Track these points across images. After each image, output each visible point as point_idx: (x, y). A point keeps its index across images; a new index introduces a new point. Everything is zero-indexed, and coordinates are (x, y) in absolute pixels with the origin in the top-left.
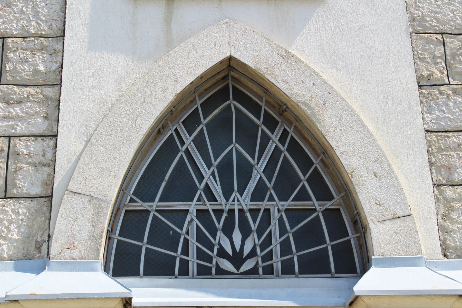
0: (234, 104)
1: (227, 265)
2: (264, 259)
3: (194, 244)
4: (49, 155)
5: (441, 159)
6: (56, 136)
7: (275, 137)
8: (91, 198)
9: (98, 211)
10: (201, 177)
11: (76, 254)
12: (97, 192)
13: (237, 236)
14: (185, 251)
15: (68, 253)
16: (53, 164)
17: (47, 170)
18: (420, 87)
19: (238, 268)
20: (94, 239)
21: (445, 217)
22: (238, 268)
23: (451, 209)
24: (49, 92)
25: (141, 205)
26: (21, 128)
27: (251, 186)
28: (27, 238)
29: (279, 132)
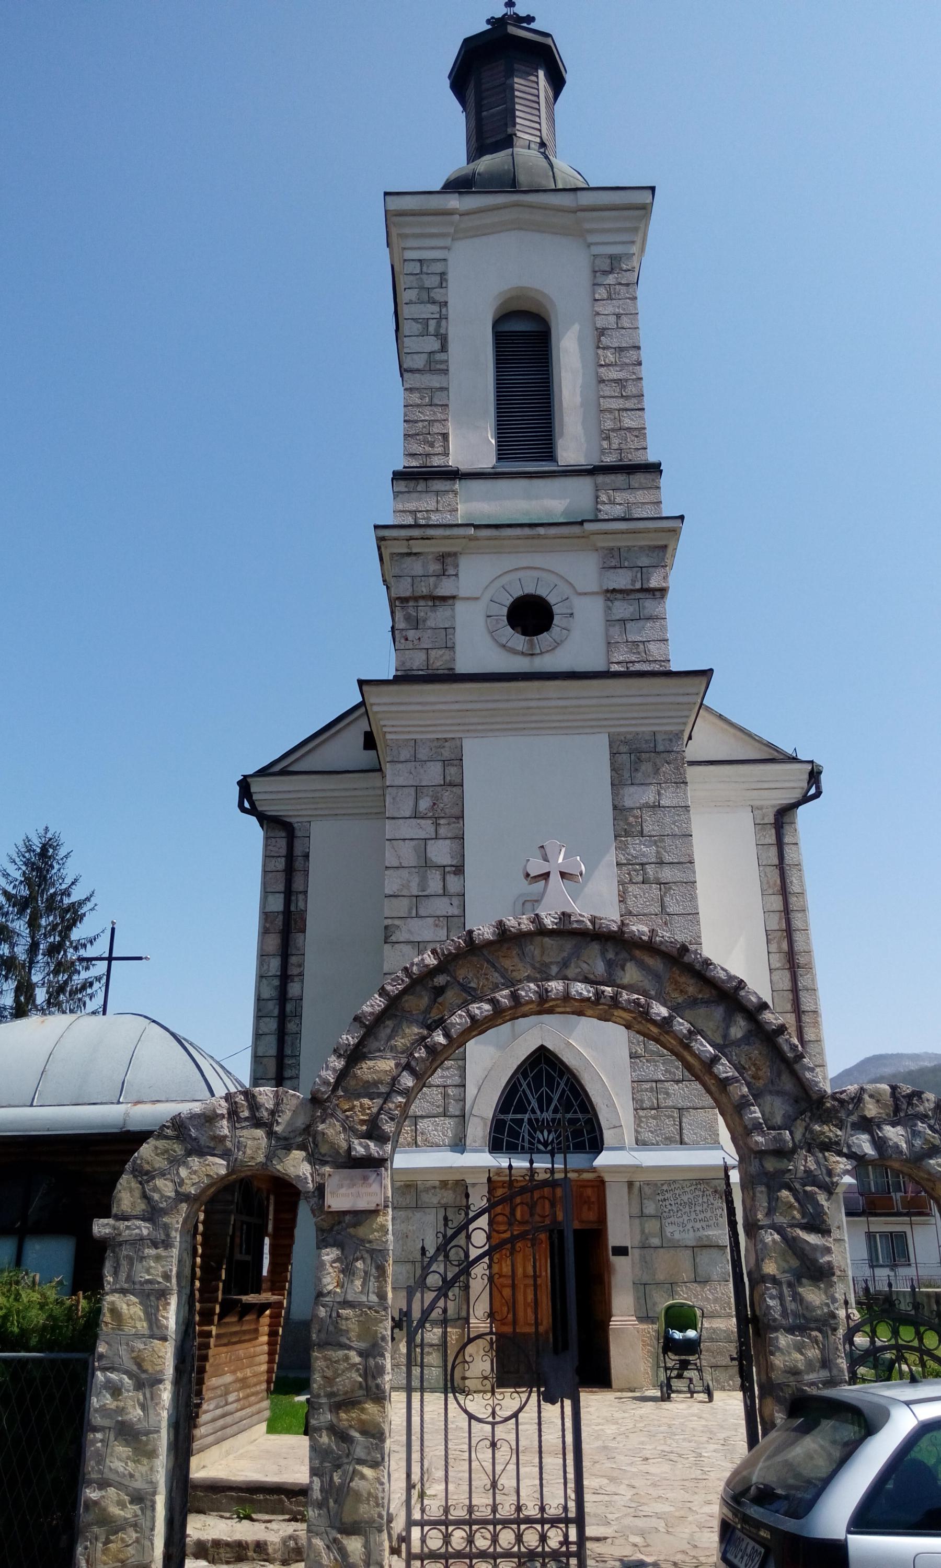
0: (544, 1066)
1: (541, 1147)
2: (558, 1144)
3: (526, 1136)
4: (462, 1095)
5: (638, 1096)
6: (464, 1086)
7: (562, 1085)
8: (482, 1118)
9: (485, 1125)
10: (529, 1103)
11: (477, 1144)
12: (485, 1116)
13: (546, 1133)
14: (523, 1141)
15: (474, 1144)
16: (464, 1100)
17: (462, 1103)
18: (631, 1058)
19: (546, 1148)
20: (484, 1137)
21: (639, 1125)
22: (546, 1148)
23: (642, 1122)
24: (460, 1063)
25: (502, 1117)
26: (449, 1082)
27: (552, 1107)
28: (455, 1135)
29: (565, 1079)
